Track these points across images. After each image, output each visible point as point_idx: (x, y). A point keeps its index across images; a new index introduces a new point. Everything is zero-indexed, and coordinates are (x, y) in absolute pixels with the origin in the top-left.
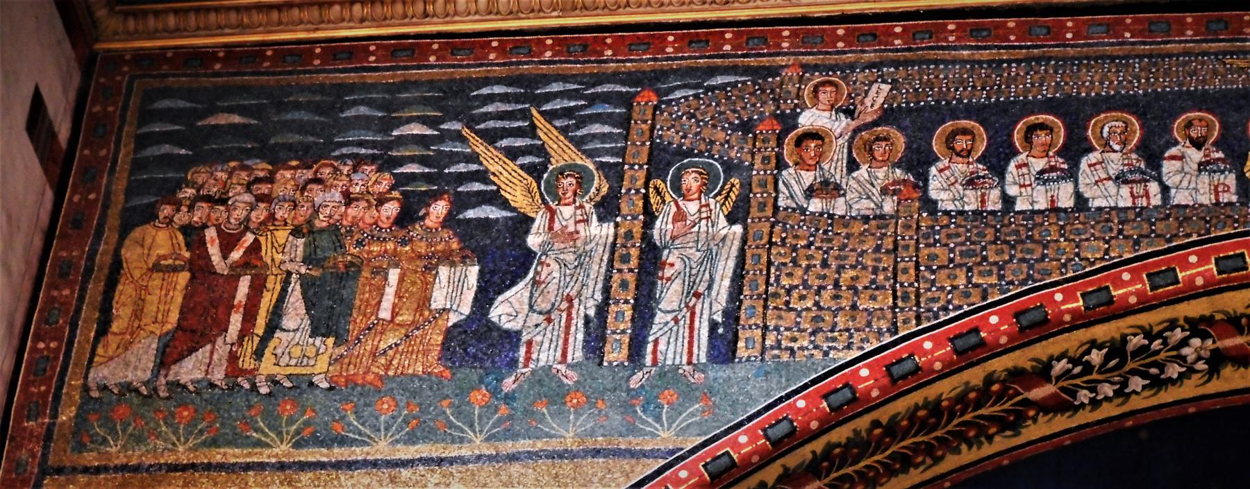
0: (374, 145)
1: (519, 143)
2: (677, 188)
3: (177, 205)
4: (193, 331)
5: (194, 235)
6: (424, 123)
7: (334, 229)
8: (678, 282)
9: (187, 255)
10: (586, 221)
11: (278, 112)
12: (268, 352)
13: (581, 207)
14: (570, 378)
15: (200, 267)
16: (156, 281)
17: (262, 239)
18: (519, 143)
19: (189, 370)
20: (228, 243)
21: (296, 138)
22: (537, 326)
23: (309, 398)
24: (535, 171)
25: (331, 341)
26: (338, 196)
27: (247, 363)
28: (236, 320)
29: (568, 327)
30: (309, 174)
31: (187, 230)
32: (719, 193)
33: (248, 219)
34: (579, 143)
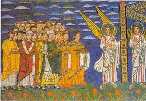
0: (59, 17)
1: (95, 17)
2: (133, 32)
3: (14, 33)
4: (24, 72)
5: (19, 42)
6: (71, 10)
7: (53, 41)
8: (137, 58)
9: (18, 49)
10: (113, 41)
11: (34, 6)
12: (43, 77)
13: (112, 36)
14: (115, 86)
15: (22, 53)
16: (12, 56)
17: (36, 44)
18: (95, 17)
19: (25, 83)
20: (28, 45)
21: (39, 14)
22: (106, 71)
23: (54, 90)
24: (100, 25)
25: (57, 75)
26: (53, 32)
27: (38, 81)
28: (34, 68)
29: (113, 71)
30: (45, 25)
31: (17, 41)
32: (143, 33)
33: (32, 38)
34: (109, 17)
